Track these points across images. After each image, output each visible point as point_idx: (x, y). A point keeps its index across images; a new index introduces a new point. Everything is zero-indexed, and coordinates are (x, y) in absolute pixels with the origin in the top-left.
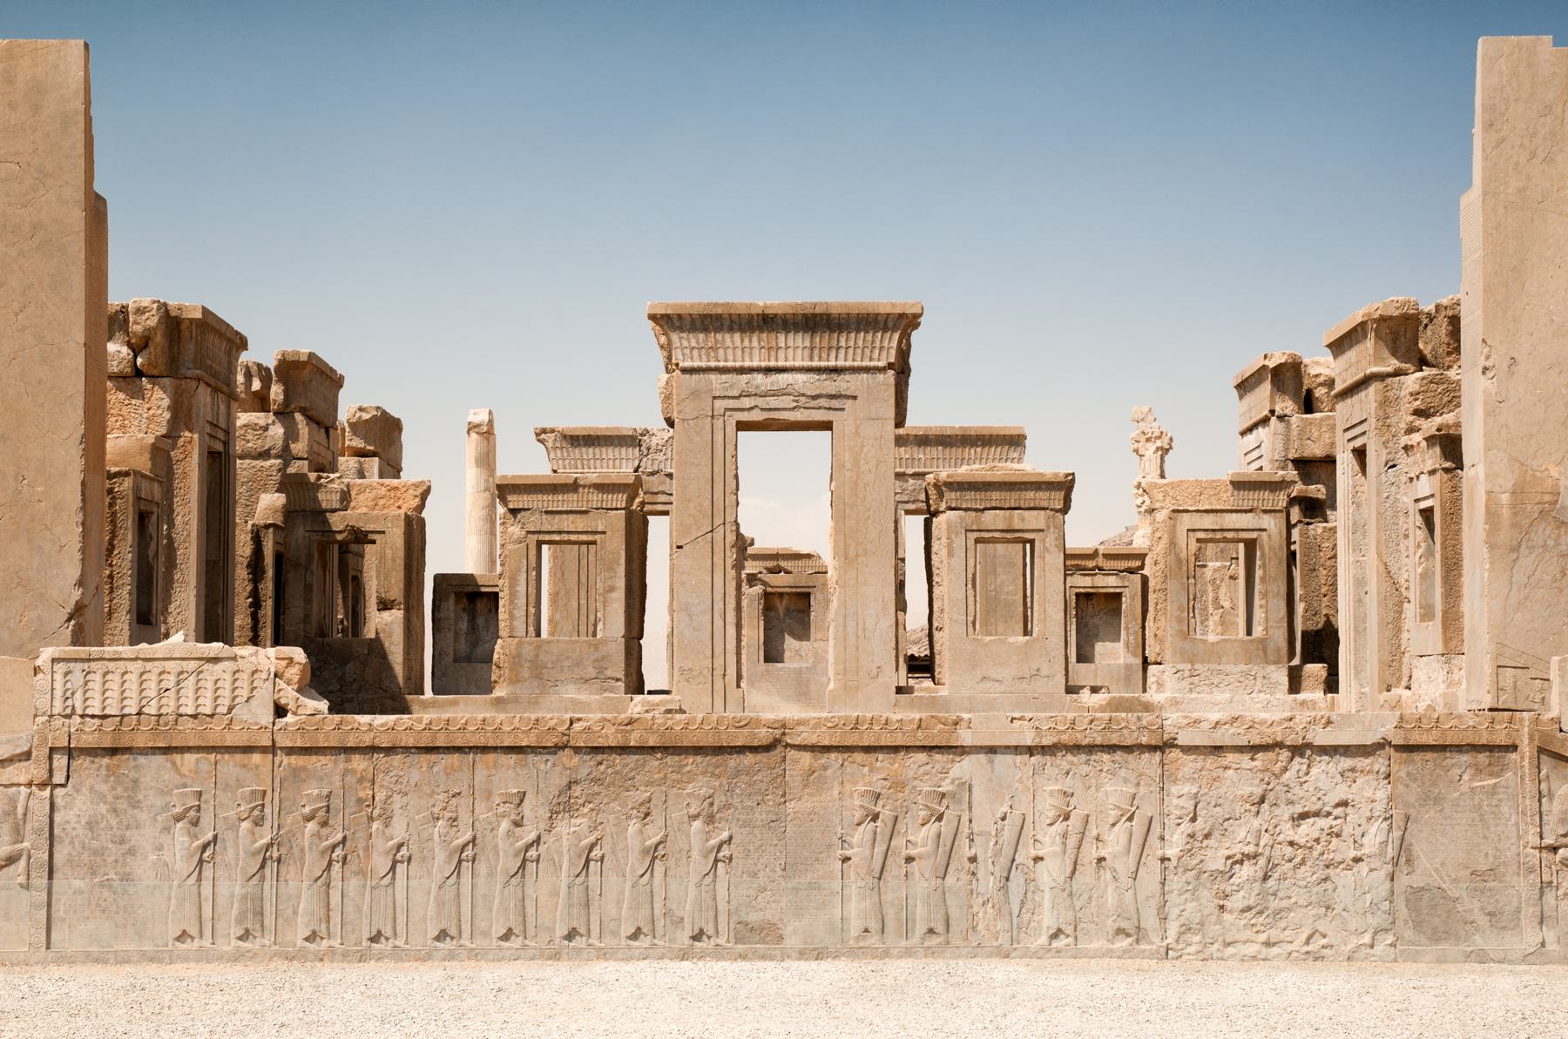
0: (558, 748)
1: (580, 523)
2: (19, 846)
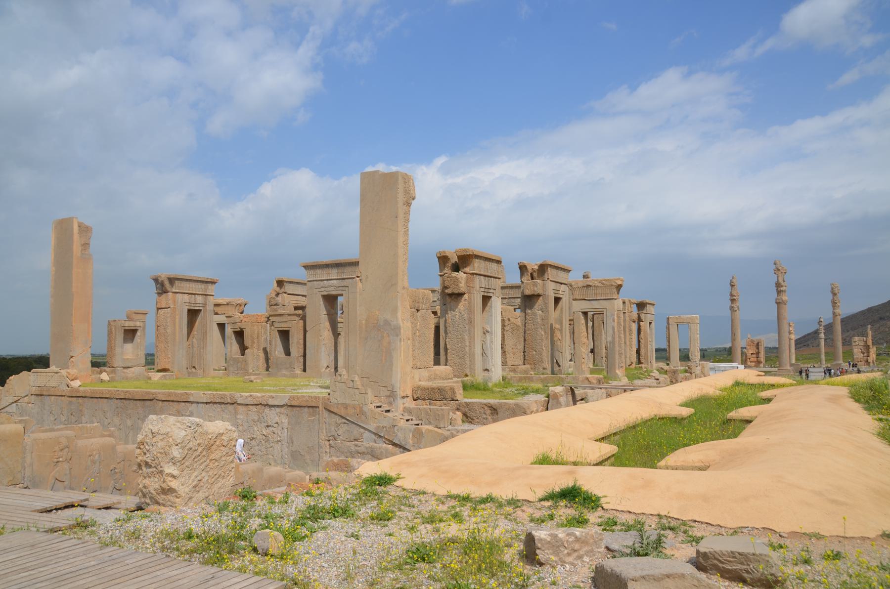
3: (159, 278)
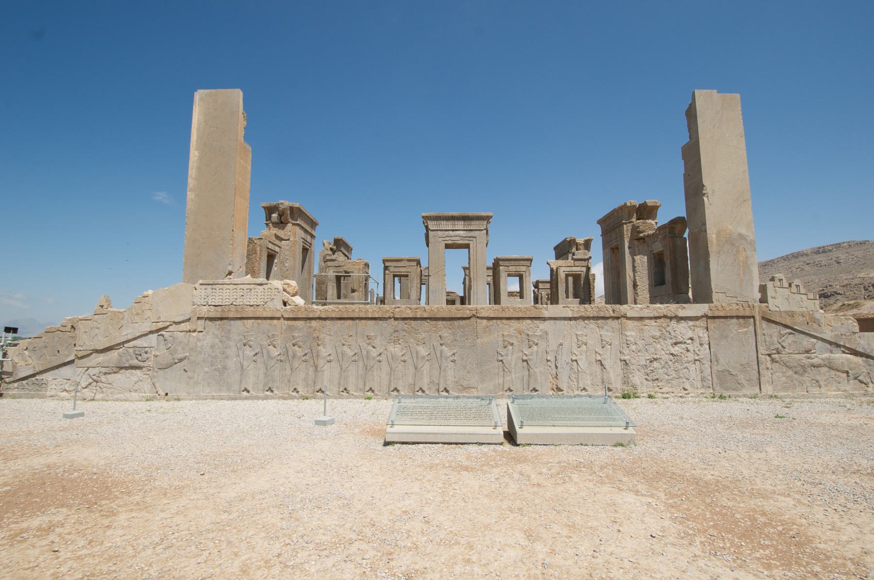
0: (390, 318)
1: (404, 270)
2: (185, 355)
3: (281, 206)
